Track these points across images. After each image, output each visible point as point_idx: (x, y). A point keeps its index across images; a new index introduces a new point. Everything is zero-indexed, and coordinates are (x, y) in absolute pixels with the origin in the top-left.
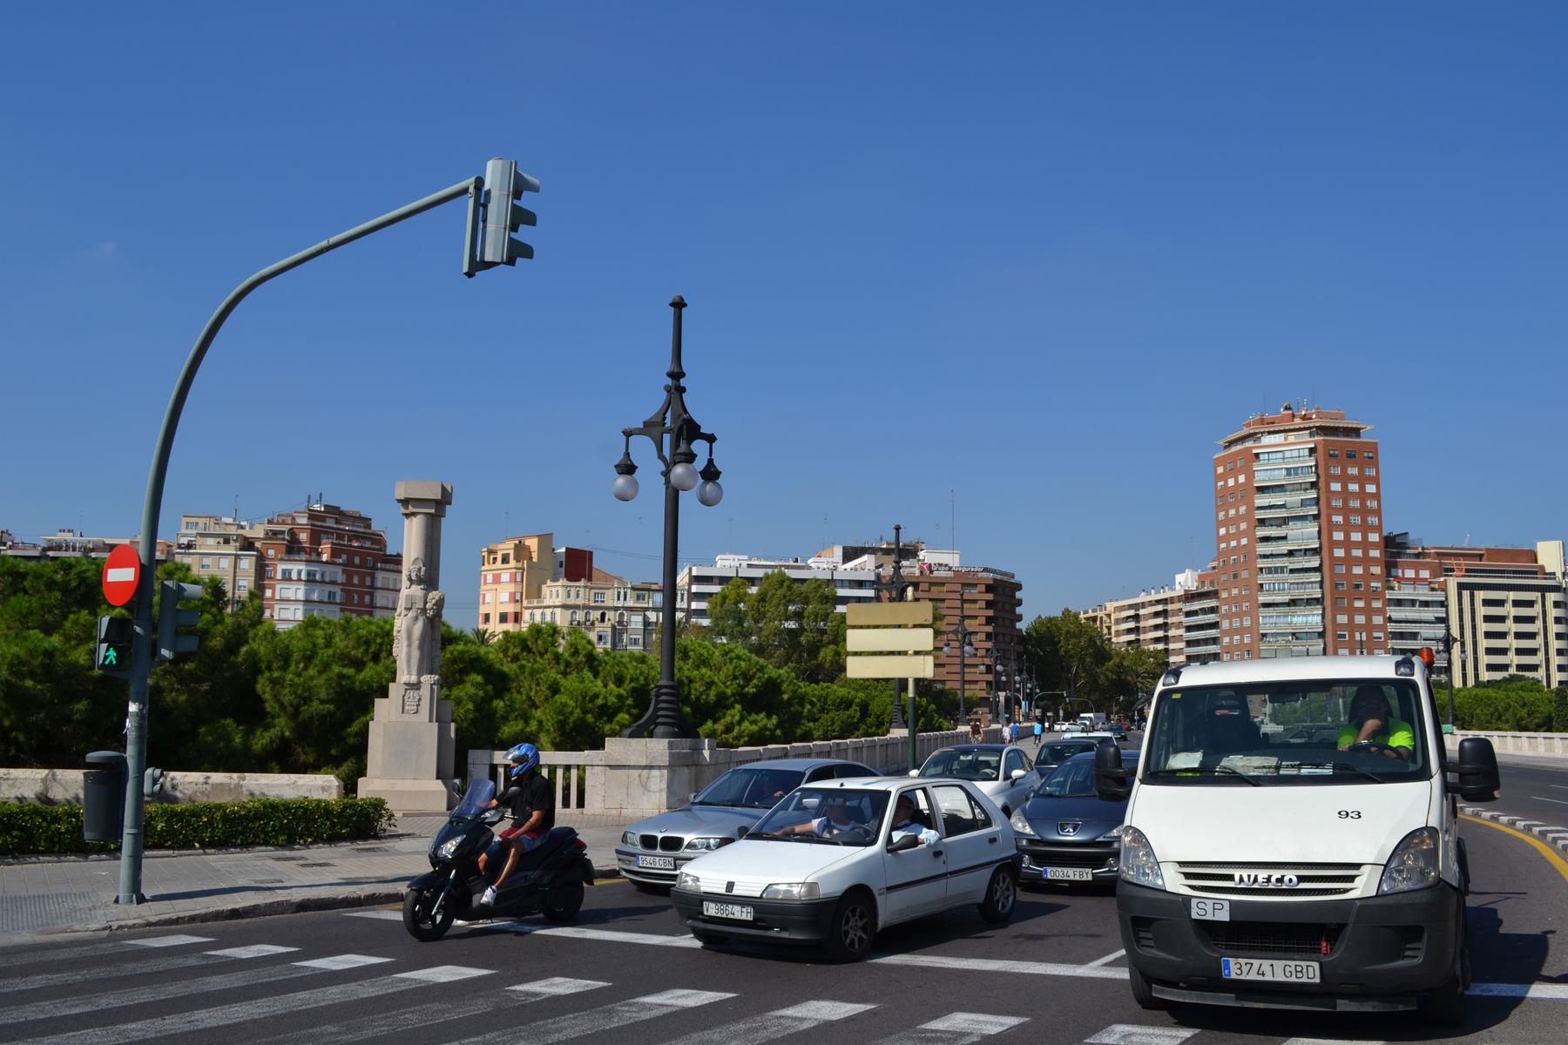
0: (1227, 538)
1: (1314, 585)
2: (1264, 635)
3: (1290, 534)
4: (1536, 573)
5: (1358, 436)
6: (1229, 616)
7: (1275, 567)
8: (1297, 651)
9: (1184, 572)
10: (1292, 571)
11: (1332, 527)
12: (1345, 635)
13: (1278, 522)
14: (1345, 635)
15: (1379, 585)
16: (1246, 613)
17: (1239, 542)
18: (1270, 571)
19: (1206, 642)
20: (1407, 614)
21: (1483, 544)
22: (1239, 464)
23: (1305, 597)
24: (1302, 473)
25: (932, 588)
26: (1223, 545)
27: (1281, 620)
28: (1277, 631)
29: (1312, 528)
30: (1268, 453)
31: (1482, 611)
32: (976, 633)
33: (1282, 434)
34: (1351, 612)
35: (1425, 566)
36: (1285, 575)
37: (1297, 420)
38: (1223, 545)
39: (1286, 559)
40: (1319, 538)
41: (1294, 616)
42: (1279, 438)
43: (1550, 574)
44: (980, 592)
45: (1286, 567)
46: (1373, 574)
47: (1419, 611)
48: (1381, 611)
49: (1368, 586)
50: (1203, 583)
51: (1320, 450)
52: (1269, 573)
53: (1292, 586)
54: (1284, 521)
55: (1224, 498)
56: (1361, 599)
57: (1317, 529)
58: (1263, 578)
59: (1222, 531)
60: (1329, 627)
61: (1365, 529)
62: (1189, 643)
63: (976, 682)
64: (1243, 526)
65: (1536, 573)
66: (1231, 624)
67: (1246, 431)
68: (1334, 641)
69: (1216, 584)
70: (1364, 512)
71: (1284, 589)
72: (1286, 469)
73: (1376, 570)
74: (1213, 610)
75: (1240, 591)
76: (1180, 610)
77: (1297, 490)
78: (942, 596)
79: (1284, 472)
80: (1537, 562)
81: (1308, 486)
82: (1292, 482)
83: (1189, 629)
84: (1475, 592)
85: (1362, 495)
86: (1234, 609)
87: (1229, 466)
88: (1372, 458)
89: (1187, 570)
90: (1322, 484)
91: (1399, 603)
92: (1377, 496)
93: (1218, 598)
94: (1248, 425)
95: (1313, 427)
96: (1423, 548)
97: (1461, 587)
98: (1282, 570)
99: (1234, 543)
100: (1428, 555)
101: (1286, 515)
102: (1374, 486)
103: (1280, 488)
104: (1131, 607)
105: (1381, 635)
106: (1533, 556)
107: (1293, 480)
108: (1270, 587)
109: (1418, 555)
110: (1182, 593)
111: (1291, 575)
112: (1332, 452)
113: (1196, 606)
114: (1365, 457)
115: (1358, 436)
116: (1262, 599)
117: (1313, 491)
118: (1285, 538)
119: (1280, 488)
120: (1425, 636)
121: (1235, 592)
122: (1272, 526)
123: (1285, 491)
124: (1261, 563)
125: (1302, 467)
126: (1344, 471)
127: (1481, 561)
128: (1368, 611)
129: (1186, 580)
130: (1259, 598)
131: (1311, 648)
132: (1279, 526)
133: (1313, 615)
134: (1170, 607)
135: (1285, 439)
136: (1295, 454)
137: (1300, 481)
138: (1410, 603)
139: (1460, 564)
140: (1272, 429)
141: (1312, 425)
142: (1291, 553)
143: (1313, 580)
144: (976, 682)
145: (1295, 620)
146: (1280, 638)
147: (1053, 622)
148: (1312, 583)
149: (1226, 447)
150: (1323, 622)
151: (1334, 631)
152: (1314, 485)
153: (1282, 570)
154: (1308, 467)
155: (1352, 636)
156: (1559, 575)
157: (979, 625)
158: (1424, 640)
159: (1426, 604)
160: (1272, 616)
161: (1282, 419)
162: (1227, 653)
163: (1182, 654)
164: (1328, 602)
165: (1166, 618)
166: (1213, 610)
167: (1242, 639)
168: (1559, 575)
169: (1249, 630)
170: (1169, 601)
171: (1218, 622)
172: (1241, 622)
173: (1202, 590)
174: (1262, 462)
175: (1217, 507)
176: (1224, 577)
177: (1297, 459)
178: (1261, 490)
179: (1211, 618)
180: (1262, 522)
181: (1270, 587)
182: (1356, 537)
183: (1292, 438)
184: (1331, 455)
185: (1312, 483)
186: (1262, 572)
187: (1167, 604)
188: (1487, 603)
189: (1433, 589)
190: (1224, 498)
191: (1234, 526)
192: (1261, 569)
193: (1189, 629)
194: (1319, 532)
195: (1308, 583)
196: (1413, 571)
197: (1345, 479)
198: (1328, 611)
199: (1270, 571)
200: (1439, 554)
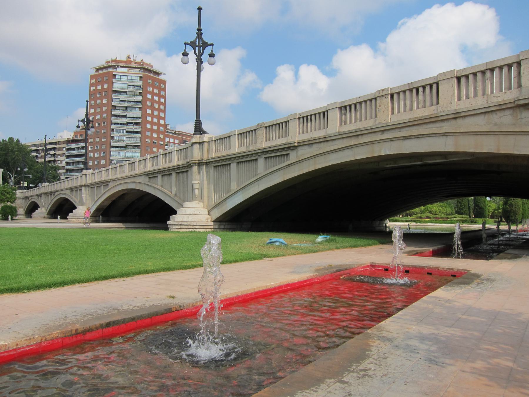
10: (128, 132)
13: (122, 108)
16: (103, 150)
17: (101, 116)
28: (119, 159)
30: (121, 75)
35: (177, 138)
42: (125, 70)
50: (76, 136)
53: (127, 139)
61: (159, 118)
64: (105, 108)
75: (101, 140)
77: (133, 95)
81: (138, 94)
86: (96, 148)
89: (65, 131)
95: (142, 68)
99: (98, 117)
101: (127, 106)
111: (128, 134)
134: (57, 146)
136: (133, 78)
140: (122, 65)
141: (141, 67)
169: (104, 158)
173: (76, 139)
182: (155, 120)
183: (132, 70)
185: (140, 93)
191: (100, 108)
196: (173, 139)
197: (153, 94)
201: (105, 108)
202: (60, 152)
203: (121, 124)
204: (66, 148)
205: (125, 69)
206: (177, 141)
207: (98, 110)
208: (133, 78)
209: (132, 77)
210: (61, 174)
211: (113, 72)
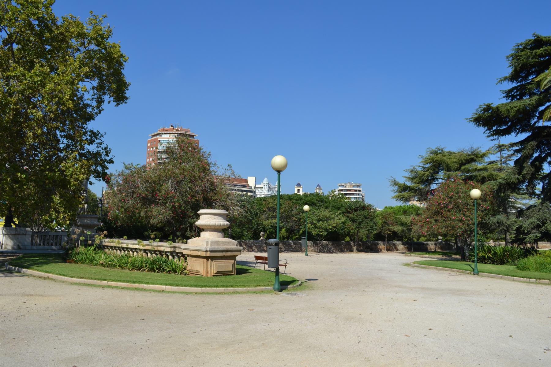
4: (246, 186)
5: (194, 138)
33: (169, 135)
37: (174, 131)
42: (167, 136)
43: (251, 187)
65: (246, 186)
67: (158, 132)
80: (247, 183)
87: (152, 144)
94: (160, 130)
106: (246, 181)
115: (194, 138)
149: (152, 137)
156: (253, 187)
161: (169, 130)
168: (253, 187)
175: (147, 157)
211: (158, 138)
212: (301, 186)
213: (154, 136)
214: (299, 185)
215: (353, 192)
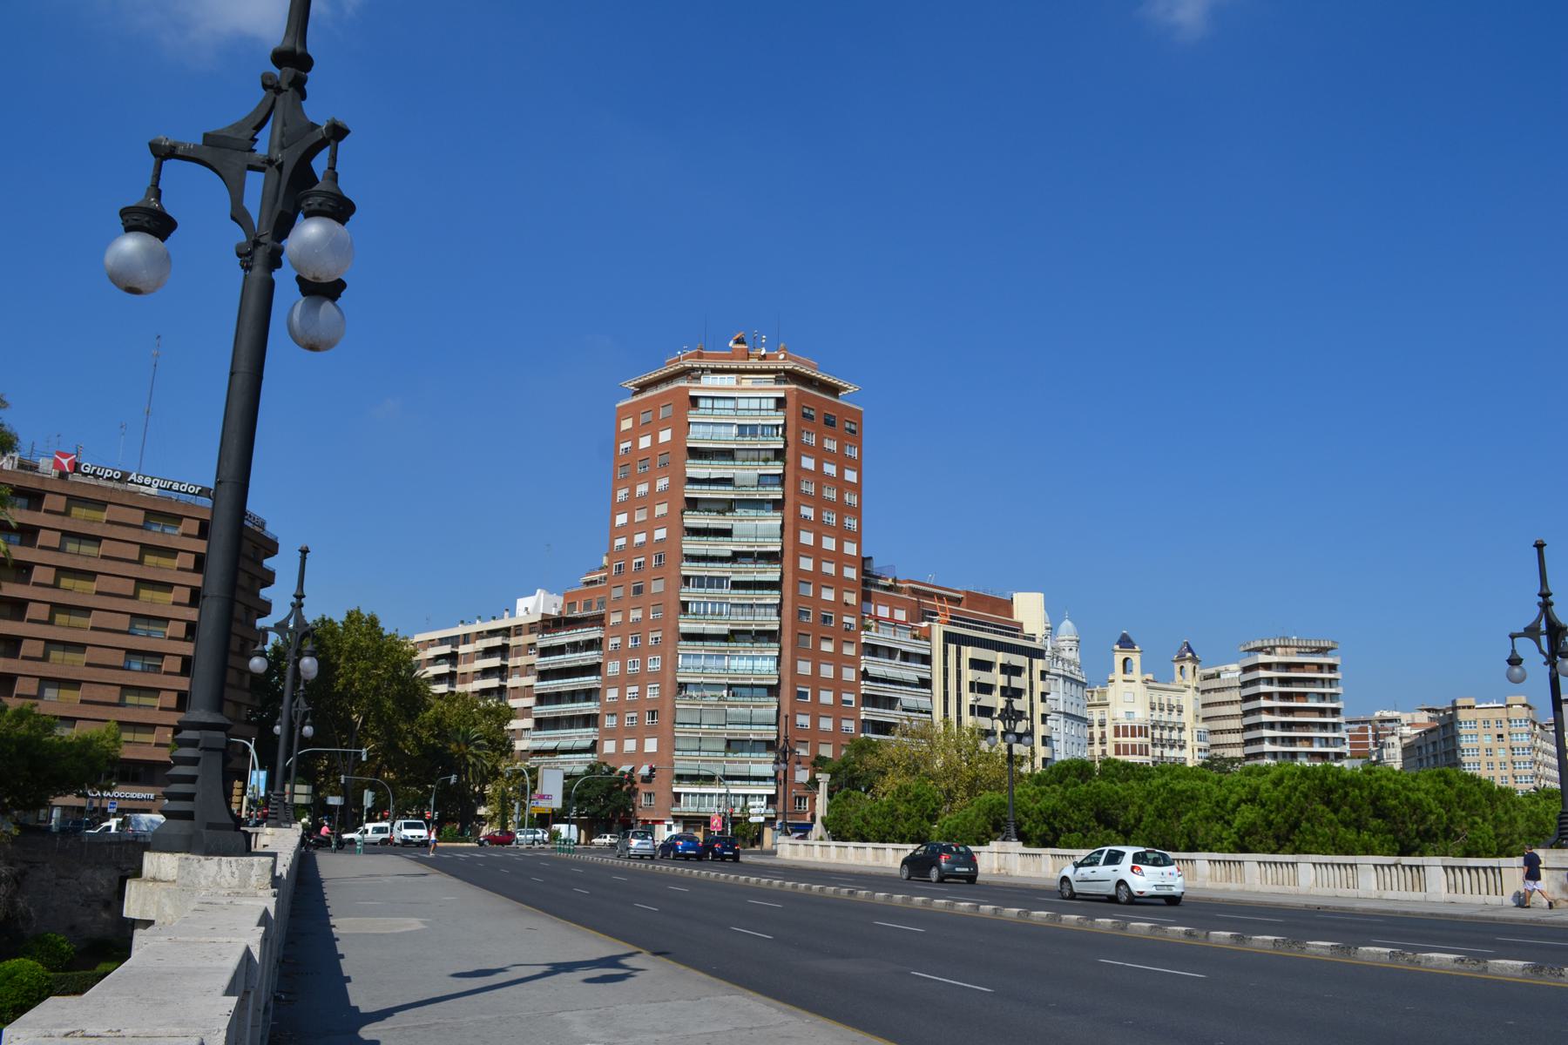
0: (629, 530)
1: (768, 610)
2: (683, 686)
3: (738, 527)
4: (1017, 630)
5: (837, 396)
6: (619, 653)
7: (710, 577)
8: (736, 716)
9: (534, 594)
10: (736, 585)
11: (800, 522)
12: (807, 693)
14: (807, 693)
15: (852, 621)
16: (654, 650)
17: (650, 536)
18: (701, 582)
19: (573, 696)
20: (886, 669)
21: (960, 587)
22: (662, 413)
23: (754, 627)
24: (763, 434)
25: (75, 511)
26: (620, 542)
27: (713, 663)
29: (771, 522)
30: (713, 398)
31: (969, 675)
32: (167, 620)
33: (734, 376)
34: (817, 658)
35: (901, 604)
36: (725, 591)
38: (620, 542)
39: (728, 565)
40: (781, 537)
41: (733, 657)
42: (729, 381)
44: (184, 535)
45: (727, 578)
46: (846, 604)
47: (900, 667)
48: (853, 662)
49: (840, 622)
50: (572, 605)
51: (791, 403)
52: (699, 586)
53: (733, 610)
54: (729, 506)
55: (632, 467)
56: (829, 639)
57: (780, 522)
58: (688, 593)
59: (621, 519)
60: (787, 679)
62: (542, 699)
63: (150, 727)
64: (661, 510)
66: (623, 667)
68: (792, 701)
69: (595, 605)
70: (841, 508)
71: (720, 614)
72: (739, 426)
73: (851, 598)
74: (591, 645)
75: (646, 615)
76: (532, 645)
77: (754, 460)
78: (96, 530)
79: (735, 430)
81: (771, 455)
82: (747, 447)
83: (544, 675)
84: (962, 647)
85: (840, 483)
87: (643, 419)
88: (854, 432)
89: (539, 591)
90: (790, 455)
91: (873, 650)
92: (857, 488)
93: (604, 626)
95: (780, 371)
96: (895, 580)
97: (949, 638)
98: (718, 582)
99: (640, 538)
100: (899, 590)
101: (733, 497)
102: (855, 474)
103: (728, 454)
104: (443, 641)
105: (851, 697)
107: (748, 442)
108: (698, 608)
109: (889, 588)
110: (538, 618)
111: (733, 592)
112: (806, 411)
113: (563, 638)
114: (846, 429)
115: (837, 396)
116: (685, 627)
117: (778, 463)
118: (727, 533)
119: (728, 454)
120: (905, 704)
121: (636, 615)
122: (710, 511)
123: (733, 459)
124: (689, 569)
125: (763, 425)
126: (820, 442)
127: (959, 606)
128: (838, 660)
129: (532, 606)
130: (680, 625)
131: (756, 711)
132: (721, 512)
133: (765, 658)
135: (738, 382)
136: (755, 404)
137: (759, 447)
138: (886, 653)
139: (943, 609)
142: (736, 557)
143: (768, 601)
144: (150, 727)
145: (735, 663)
146: (707, 693)
147: (328, 626)
148: (766, 606)
149: (636, 393)
150: (777, 669)
151: (794, 686)
152: (779, 454)
153: (718, 582)
154: (772, 426)
155: (816, 696)
157: (174, 603)
158: (903, 710)
159: (906, 656)
160: (699, 656)
162: (612, 715)
163: (529, 716)
164: (787, 638)
165: (504, 658)
166: (591, 645)
167: (642, 692)
169: (657, 676)
170: (512, 632)
171: (599, 664)
172: (644, 665)
174: (701, 411)
176: (617, 593)
177: (757, 413)
178: (696, 453)
179: (589, 657)
180: (693, 504)
181: (698, 608)
182: (829, 544)
183: (747, 381)
184: (804, 415)
185: (777, 451)
186: (687, 584)
187: (508, 636)
188: (976, 664)
189: (915, 637)
190: (632, 467)
192: (686, 579)
193: (544, 675)
194: (782, 527)
195: (760, 606)
196: (888, 609)
197: (821, 455)
198: (787, 654)
199: (701, 582)
200: (915, 592)
201: (661, 510)
202: (521, 661)
203: (713, 559)
204: (539, 645)
205: (726, 376)
206: (901, 615)
207: (640, 516)
208: (755, 404)
209: (751, 400)
210: (519, 733)
211: (687, 389)
212: (1137, 648)
213: (643, 388)
214: (1126, 643)
215: (1313, 672)
